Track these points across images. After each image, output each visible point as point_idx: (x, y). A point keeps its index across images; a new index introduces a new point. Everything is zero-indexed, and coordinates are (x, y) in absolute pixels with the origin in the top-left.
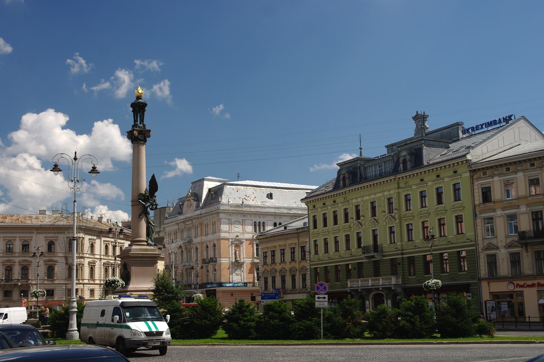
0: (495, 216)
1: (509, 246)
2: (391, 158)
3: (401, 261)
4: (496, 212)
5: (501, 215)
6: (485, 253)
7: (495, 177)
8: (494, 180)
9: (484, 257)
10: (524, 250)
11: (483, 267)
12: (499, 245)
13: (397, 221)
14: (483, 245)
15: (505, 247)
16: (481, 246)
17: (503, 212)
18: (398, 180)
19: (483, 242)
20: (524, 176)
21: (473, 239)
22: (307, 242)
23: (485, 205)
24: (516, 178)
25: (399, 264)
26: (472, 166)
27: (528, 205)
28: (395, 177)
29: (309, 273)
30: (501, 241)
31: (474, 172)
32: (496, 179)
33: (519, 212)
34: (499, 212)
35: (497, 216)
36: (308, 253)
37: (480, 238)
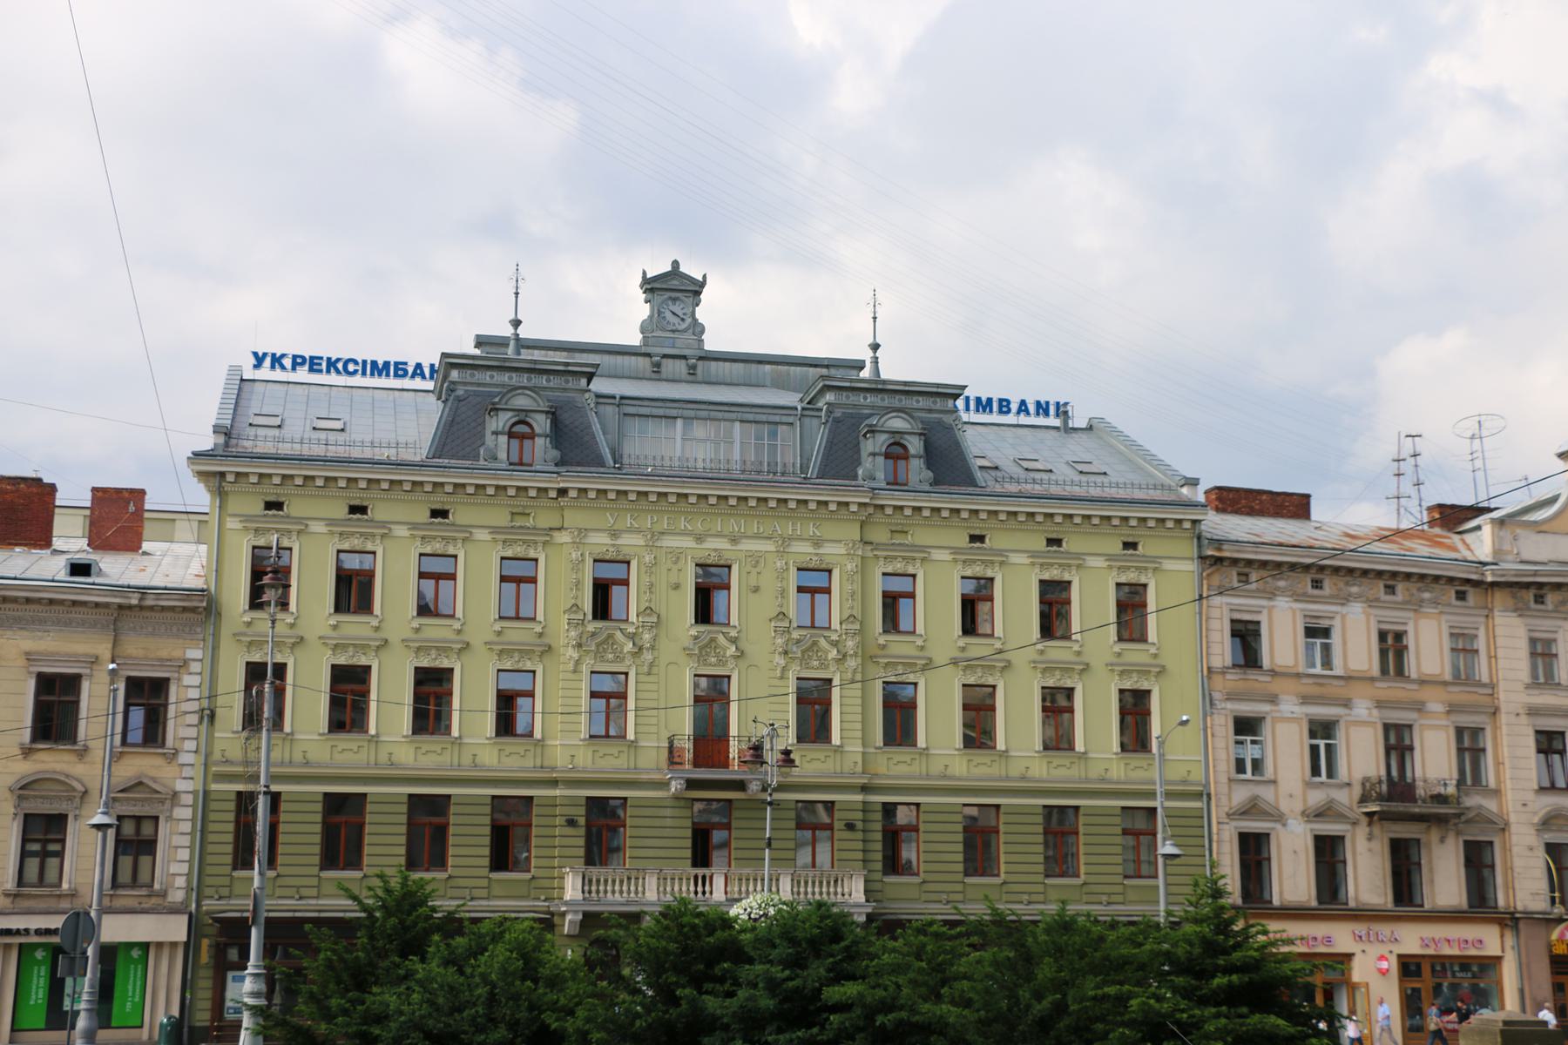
0: (1275, 715)
1: (1320, 814)
2: (791, 420)
3: (860, 815)
5: (1295, 716)
7: (1280, 598)
8: (1272, 603)
10: (1362, 831)
12: (1284, 806)
13: (852, 663)
18: (871, 510)
19: (1230, 787)
20: (1368, 616)
22: (186, 663)
23: (1242, 677)
24: (1343, 617)
25: (850, 827)
26: (1225, 547)
27: (1380, 704)
28: (871, 499)
29: (188, 813)
30: (1291, 796)
31: (1215, 563)
32: (1283, 604)
34: (1289, 706)
35: (1278, 715)
36: (194, 719)
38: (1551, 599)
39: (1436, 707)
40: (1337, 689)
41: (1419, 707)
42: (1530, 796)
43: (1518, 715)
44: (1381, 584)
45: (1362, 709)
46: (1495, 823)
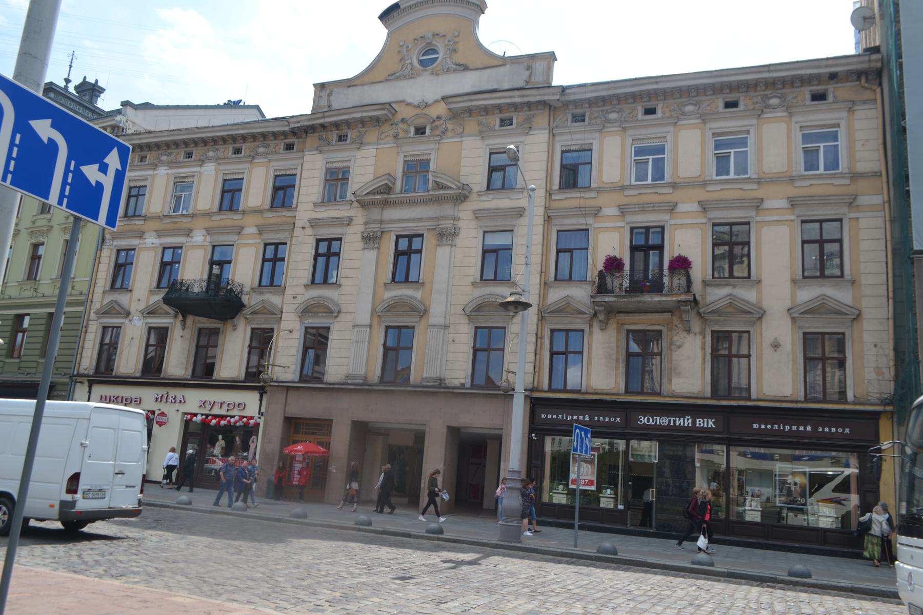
0: (140, 246)
1: (151, 312)
4: (145, 239)
5: (153, 245)
6: (100, 323)
7: (160, 168)
8: (156, 172)
9: (97, 329)
11: (90, 351)
14: (101, 304)
15: (143, 314)
16: (96, 306)
17: (157, 241)
21: (85, 291)
24: (200, 173)
27: (209, 231)
30: (139, 300)
33: (188, 244)
35: (144, 246)
37: (99, 290)
38: (351, 135)
39: (251, 230)
40: (185, 223)
41: (239, 230)
42: (301, 290)
43: (303, 228)
44: (230, 148)
45: (199, 237)
46: (276, 314)
